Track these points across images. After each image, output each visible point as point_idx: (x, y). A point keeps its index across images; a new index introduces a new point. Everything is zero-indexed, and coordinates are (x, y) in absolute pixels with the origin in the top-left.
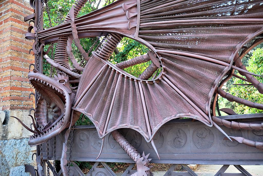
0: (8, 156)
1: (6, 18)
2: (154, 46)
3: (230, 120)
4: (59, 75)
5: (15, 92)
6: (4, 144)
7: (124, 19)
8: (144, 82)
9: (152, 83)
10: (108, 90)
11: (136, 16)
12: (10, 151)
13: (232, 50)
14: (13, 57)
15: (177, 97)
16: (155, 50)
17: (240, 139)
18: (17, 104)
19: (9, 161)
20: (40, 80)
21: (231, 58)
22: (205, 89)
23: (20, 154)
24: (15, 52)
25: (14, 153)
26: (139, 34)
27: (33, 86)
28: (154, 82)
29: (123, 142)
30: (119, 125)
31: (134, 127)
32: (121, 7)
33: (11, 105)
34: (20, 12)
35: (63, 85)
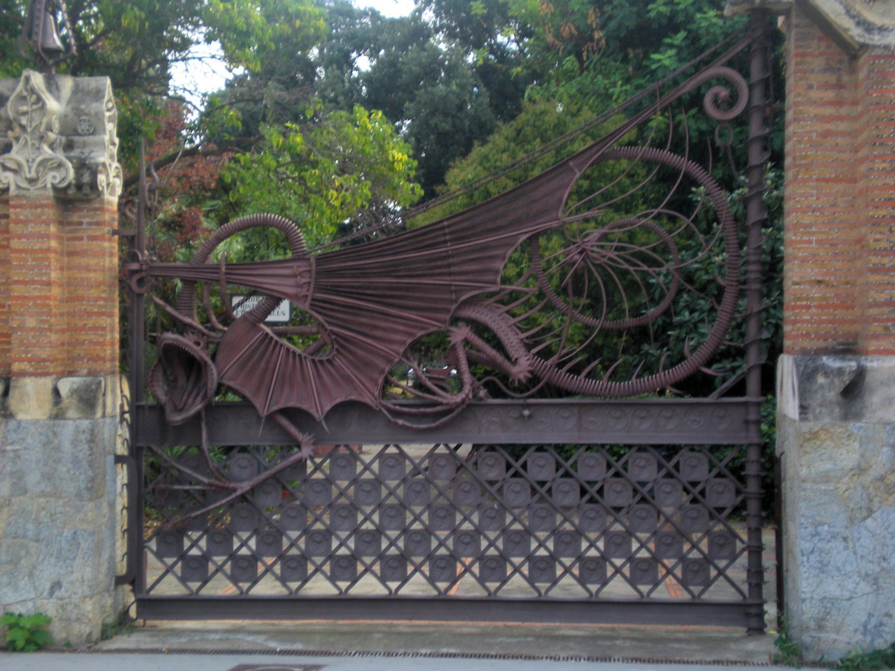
1: (91, 233)
2: (327, 322)
3: (395, 405)
4: (190, 335)
7: (291, 281)
8: (313, 361)
9: (321, 362)
10: (268, 362)
11: (309, 283)
13: (403, 343)
15: (348, 380)
16: (329, 327)
17: (400, 422)
21: (402, 350)
22: (375, 375)
26: (311, 305)
29: (284, 422)
30: (281, 405)
31: (305, 407)
32: (292, 267)
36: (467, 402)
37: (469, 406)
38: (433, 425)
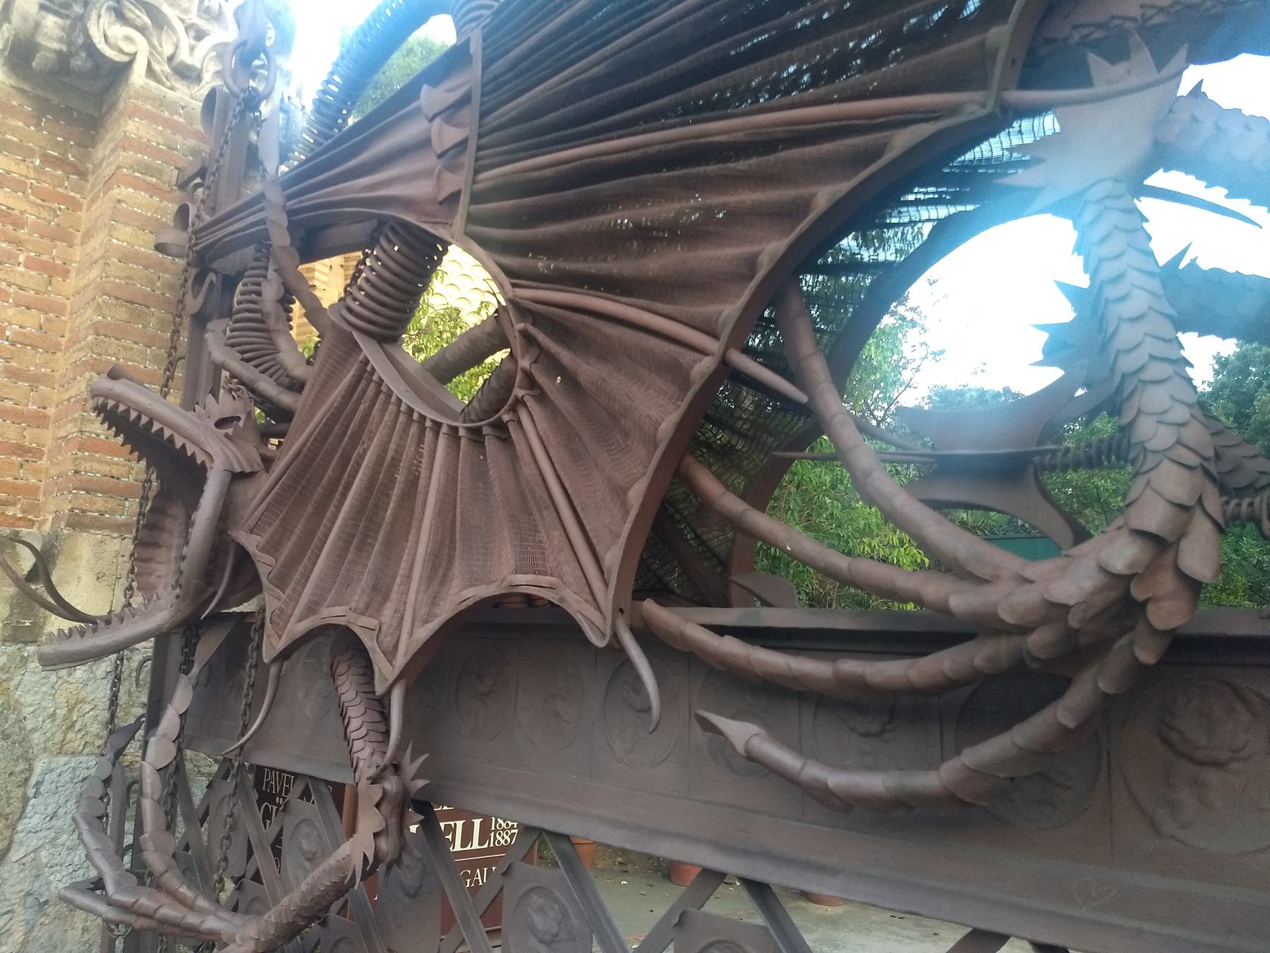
0: (32, 709)
5: (99, 461)
6: (23, 657)
12: (44, 689)
14: (109, 323)
18: (102, 509)
19: (33, 730)
20: (127, 411)
23: (87, 707)
24: (121, 305)
25: (61, 700)
26: (471, 219)
27: (116, 435)
28: (486, 430)
33: (72, 510)
34: (161, 150)
35: (226, 435)
36: (1168, 613)
37: (1187, 650)
38: (928, 781)
